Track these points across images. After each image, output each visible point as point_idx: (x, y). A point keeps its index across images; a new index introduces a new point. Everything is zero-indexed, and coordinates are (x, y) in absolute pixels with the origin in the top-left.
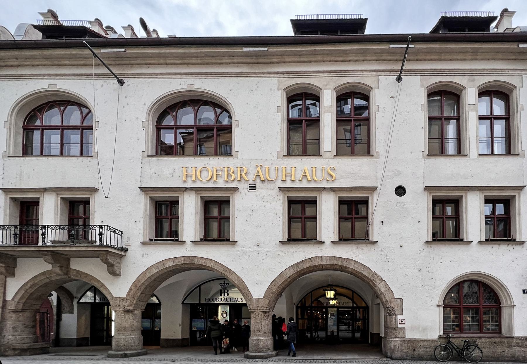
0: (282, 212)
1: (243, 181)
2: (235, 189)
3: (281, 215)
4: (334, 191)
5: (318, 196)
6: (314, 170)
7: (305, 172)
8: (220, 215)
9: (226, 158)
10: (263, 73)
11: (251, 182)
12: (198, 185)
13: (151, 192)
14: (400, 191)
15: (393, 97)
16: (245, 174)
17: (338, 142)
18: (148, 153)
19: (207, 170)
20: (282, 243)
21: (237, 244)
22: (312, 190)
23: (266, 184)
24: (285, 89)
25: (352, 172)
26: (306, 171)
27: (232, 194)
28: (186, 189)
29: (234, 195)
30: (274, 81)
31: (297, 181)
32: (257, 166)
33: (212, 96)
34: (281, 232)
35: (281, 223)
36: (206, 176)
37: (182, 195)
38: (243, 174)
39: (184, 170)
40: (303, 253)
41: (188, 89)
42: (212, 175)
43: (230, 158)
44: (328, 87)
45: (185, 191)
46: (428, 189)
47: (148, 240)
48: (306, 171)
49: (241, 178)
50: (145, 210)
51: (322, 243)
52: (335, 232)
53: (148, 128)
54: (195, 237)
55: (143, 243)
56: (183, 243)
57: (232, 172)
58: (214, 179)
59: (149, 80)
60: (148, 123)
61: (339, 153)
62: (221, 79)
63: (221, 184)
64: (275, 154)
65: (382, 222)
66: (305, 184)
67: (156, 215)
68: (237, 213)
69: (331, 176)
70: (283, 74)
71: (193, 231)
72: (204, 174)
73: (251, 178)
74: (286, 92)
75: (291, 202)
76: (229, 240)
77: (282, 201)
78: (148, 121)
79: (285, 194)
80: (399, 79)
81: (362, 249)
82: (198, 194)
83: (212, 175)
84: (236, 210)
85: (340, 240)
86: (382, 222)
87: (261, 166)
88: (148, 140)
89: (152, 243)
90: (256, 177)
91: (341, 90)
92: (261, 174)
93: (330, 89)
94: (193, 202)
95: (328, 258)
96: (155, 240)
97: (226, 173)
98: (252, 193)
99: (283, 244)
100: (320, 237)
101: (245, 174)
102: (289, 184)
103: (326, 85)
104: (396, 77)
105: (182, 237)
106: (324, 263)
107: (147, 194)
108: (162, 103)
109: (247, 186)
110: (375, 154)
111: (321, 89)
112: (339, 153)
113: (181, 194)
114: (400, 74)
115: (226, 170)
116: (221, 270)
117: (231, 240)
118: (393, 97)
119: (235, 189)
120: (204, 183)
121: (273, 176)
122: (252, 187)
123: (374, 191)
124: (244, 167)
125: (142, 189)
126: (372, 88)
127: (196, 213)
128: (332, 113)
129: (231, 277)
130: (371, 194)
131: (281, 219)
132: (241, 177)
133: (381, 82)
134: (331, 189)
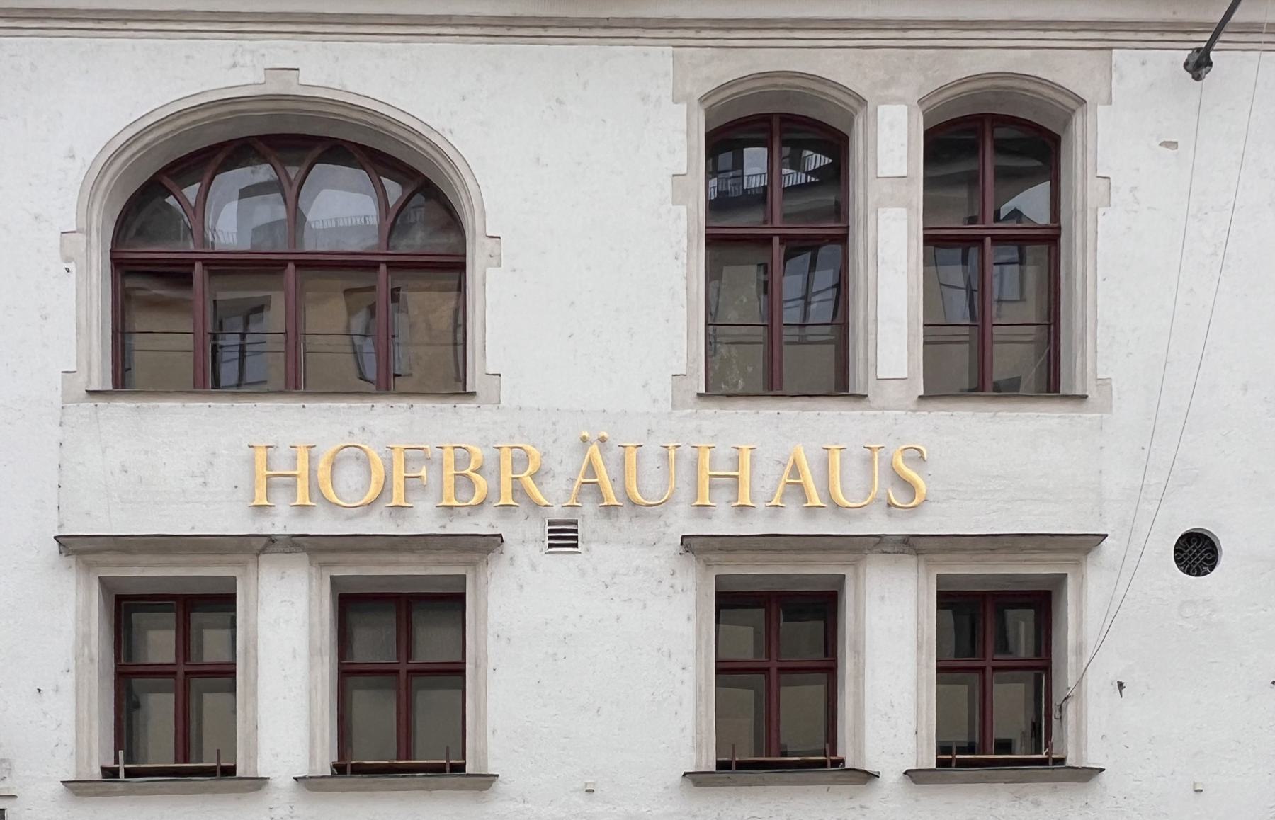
0: (692, 647)
1: (523, 507)
2: (489, 544)
3: (690, 660)
4: (918, 553)
5: (848, 572)
6: (836, 458)
7: (795, 472)
8: (409, 656)
9: (446, 406)
10: (608, 24)
11: (557, 513)
12: (321, 524)
13: (111, 558)
14: (1197, 552)
15: (1172, 145)
16: (533, 476)
17: (935, 335)
18: (89, 381)
19: (366, 463)
20: (696, 778)
21: (498, 786)
22: (826, 549)
23: (624, 521)
24: (703, 100)
25: (992, 472)
26: (796, 465)
27: (474, 564)
28: (269, 544)
29: (481, 568)
30: (657, 59)
31: (761, 506)
32: (584, 439)
33: (375, 122)
34: (690, 730)
35: (688, 693)
36: (351, 487)
37: (251, 567)
39: (261, 455)
41: (273, 88)
42: (387, 479)
43: (465, 407)
44: (893, 91)
45: (263, 551)
47: (97, 774)
48: (796, 465)
50: (84, 638)
51: (868, 777)
52: (923, 733)
53: (89, 261)
54: (312, 758)
55: (77, 788)
56: (258, 783)
57: (472, 467)
58: (398, 498)
59: (85, 44)
60: (88, 243)
61: (937, 389)
62: (421, 49)
63: (424, 521)
64: (663, 388)
65: (1121, 685)
66: (792, 523)
67: (117, 658)
68: (494, 650)
69: (908, 486)
71: (301, 732)
72: (350, 475)
73: (556, 497)
74: (708, 112)
75: (731, 601)
76: (460, 768)
77: (692, 596)
78: (88, 233)
79: (708, 565)
80: (1199, 65)
81: (1037, 804)
82: (323, 565)
83: (387, 479)
84: (490, 639)
85: (941, 763)
86: (1121, 685)
87: (603, 440)
88: (89, 326)
89: (119, 787)
90: (580, 493)
91: (947, 104)
92: (604, 477)
93: (900, 100)
94: (301, 604)
96: (129, 773)
97: (450, 472)
98: (563, 562)
100: (860, 751)
102: (723, 524)
103: (886, 85)
104: (1183, 56)
105: (252, 756)
107: (89, 566)
108: (150, 149)
109: (540, 531)
110: (1091, 392)
111: (862, 101)
112: (937, 389)
113: (243, 565)
115: (449, 459)
117: (469, 769)
118: (1172, 145)
119: (489, 544)
120: (349, 518)
121: (648, 487)
122: (563, 536)
123: (1087, 551)
124: (529, 448)
125: (69, 545)
126: (1082, 102)
127: (313, 652)
128: (909, 206)
130: (1078, 564)
131: (689, 677)
132: (519, 489)
133: (1121, 77)
134: (910, 545)
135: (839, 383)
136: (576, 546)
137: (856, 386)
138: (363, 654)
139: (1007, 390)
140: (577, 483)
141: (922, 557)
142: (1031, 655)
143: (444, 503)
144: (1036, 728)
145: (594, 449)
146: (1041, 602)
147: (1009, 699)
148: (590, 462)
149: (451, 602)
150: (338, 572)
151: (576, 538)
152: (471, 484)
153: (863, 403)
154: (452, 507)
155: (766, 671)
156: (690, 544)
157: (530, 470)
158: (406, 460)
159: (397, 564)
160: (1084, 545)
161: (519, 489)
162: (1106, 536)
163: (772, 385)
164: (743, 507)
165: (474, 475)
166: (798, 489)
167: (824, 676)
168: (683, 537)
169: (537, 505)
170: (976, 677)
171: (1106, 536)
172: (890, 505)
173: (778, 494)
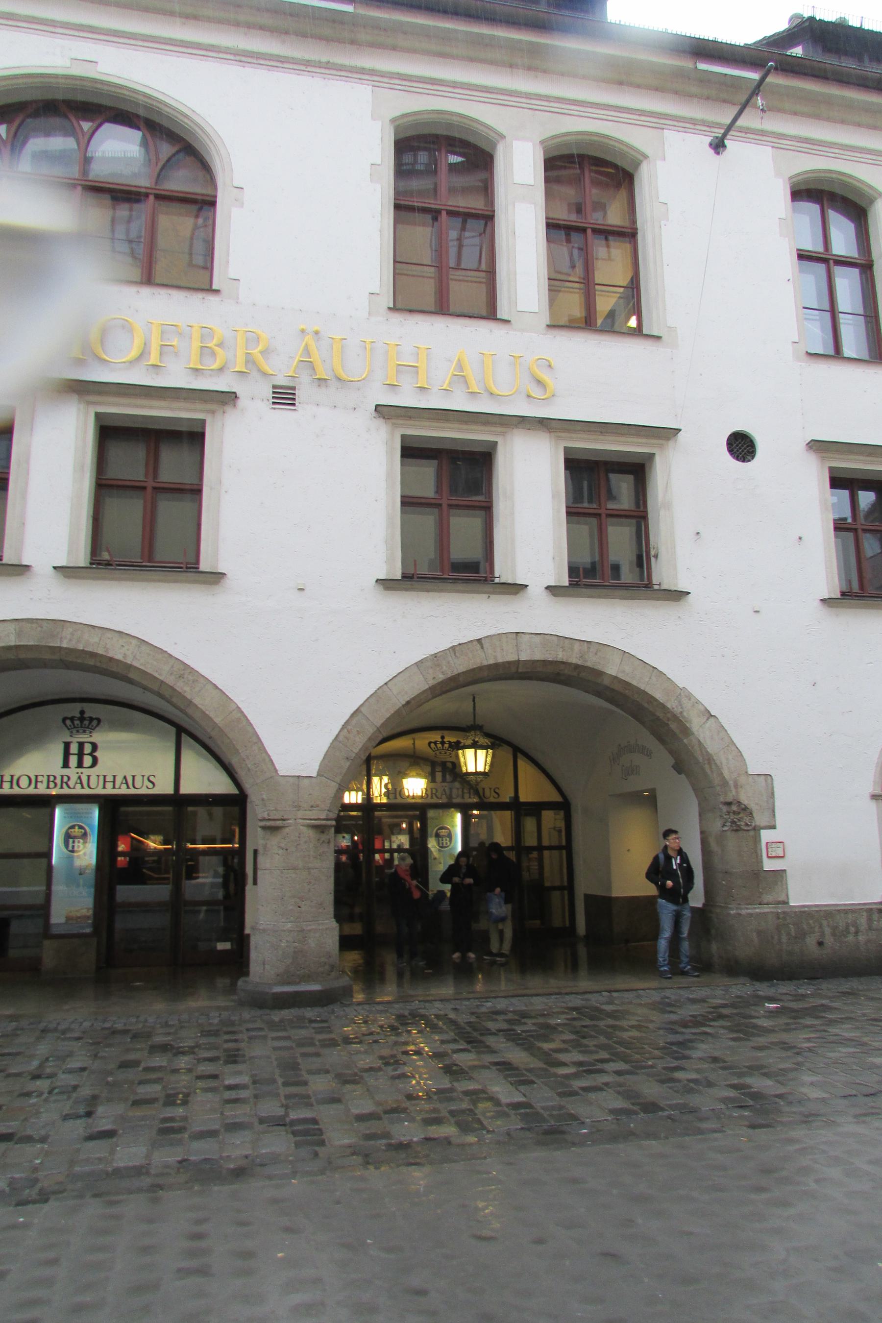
1: (255, 373)
5: (499, 440)
14: (741, 446)
38: (255, 352)
40: (450, 626)
42: (146, 345)
43: (212, 299)
46: (818, 447)
48: (457, 365)
49: (247, 362)
57: (215, 341)
58: (154, 359)
63: (176, 377)
69: (540, 383)
70: (391, 78)
83: (146, 345)
90: (297, 367)
95: (537, 639)
97: (196, 344)
98: (283, 414)
99: (387, 588)
101: (261, 352)
106: (524, 657)
114: (724, 135)
116: (164, 674)
122: (284, 397)
129: (197, 701)
132: (250, 360)
134: (544, 424)
135: (490, 313)
136: (294, 405)
137: (502, 313)
138: (115, 472)
139: (611, 326)
140: (297, 360)
141: (553, 434)
142: (633, 507)
143: (192, 366)
144: (640, 558)
145: (308, 339)
146: (638, 470)
147: (620, 537)
148: (306, 345)
149: (193, 438)
150: (102, 409)
151: (294, 399)
152: (213, 354)
153: (506, 326)
154: (197, 370)
155: (438, 506)
156: (381, 411)
157: (260, 348)
158: (162, 332)
159: (151, 407)
160: (666, 434)
161: (250, 360)
162: (680, 430)
163: (442, 307)
164: (422, 388)
165: (216, 348)
166: (461, 378)
167: (483, 513)
168: (377, 406)
169: (265, 374)
170: (594, 521)
171: (680, 430)
172: (529, 396)
173: (447, 382)
